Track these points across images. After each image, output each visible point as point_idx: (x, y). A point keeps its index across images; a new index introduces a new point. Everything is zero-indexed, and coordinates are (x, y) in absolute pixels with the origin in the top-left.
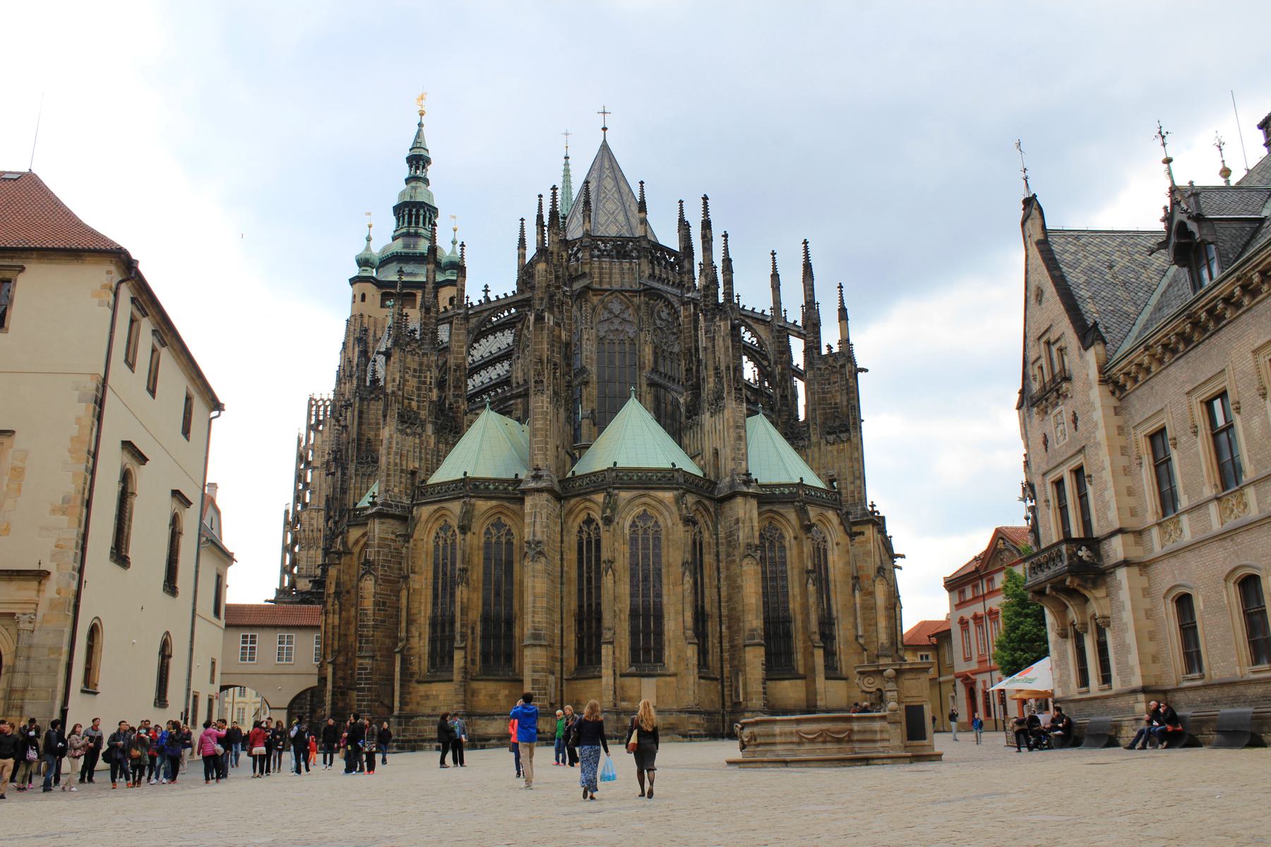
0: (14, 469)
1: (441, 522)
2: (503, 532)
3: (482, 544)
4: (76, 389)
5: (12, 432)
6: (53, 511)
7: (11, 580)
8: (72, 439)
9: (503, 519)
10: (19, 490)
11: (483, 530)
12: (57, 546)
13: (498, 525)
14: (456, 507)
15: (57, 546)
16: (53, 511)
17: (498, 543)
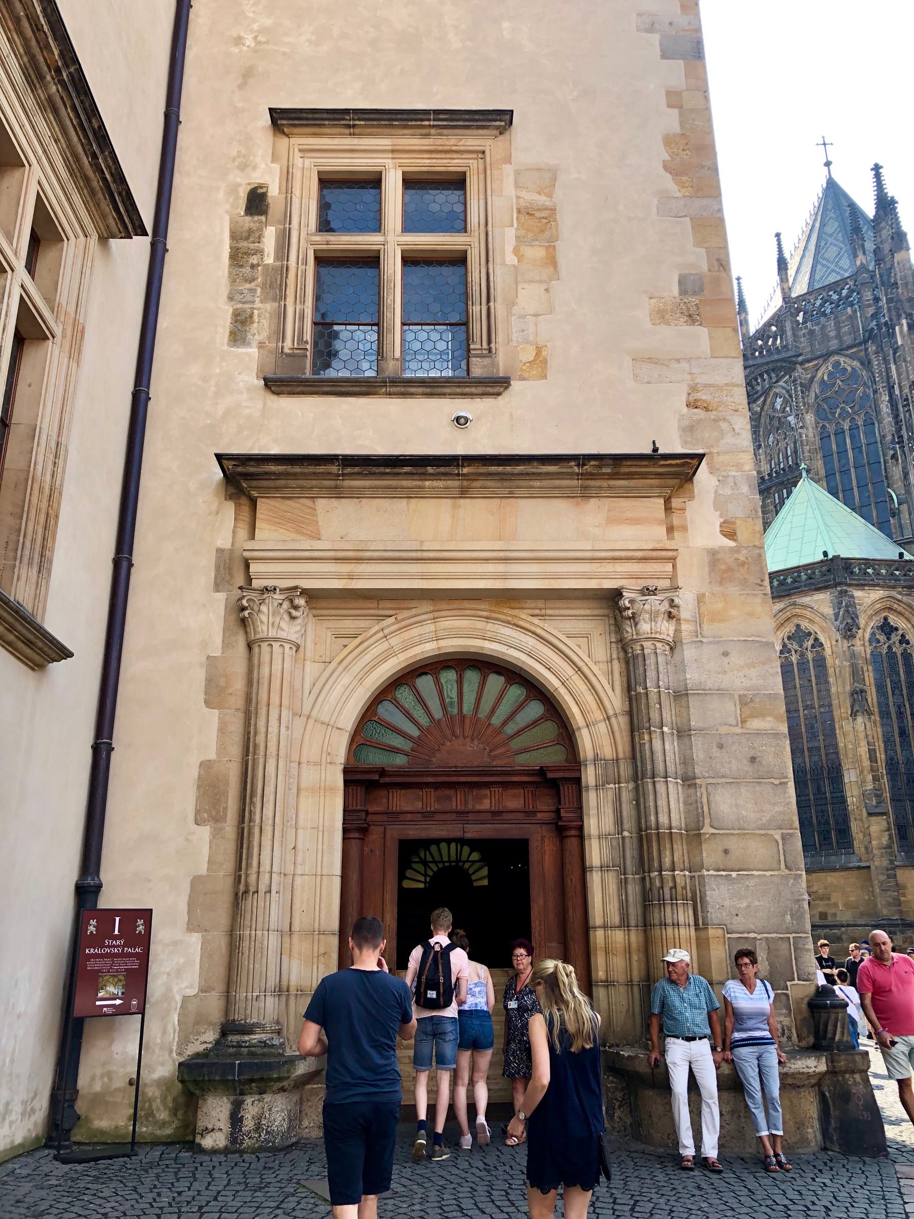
0: (526, 212)
1: (790, 628)
2: (895, 638)
3: (868, 657)
4: (651, 29)
5: (501, 120)
6: (661, 316)
7: (585, 494)
8: (668, 141)
9: (894, 620)
10: (552, 261)
11: (867, 636)
12: (693, 405)
13: (887, 628)
14: (822, 602)
15: (693, 405)
16: (661, 316)
17: (891, 654)
